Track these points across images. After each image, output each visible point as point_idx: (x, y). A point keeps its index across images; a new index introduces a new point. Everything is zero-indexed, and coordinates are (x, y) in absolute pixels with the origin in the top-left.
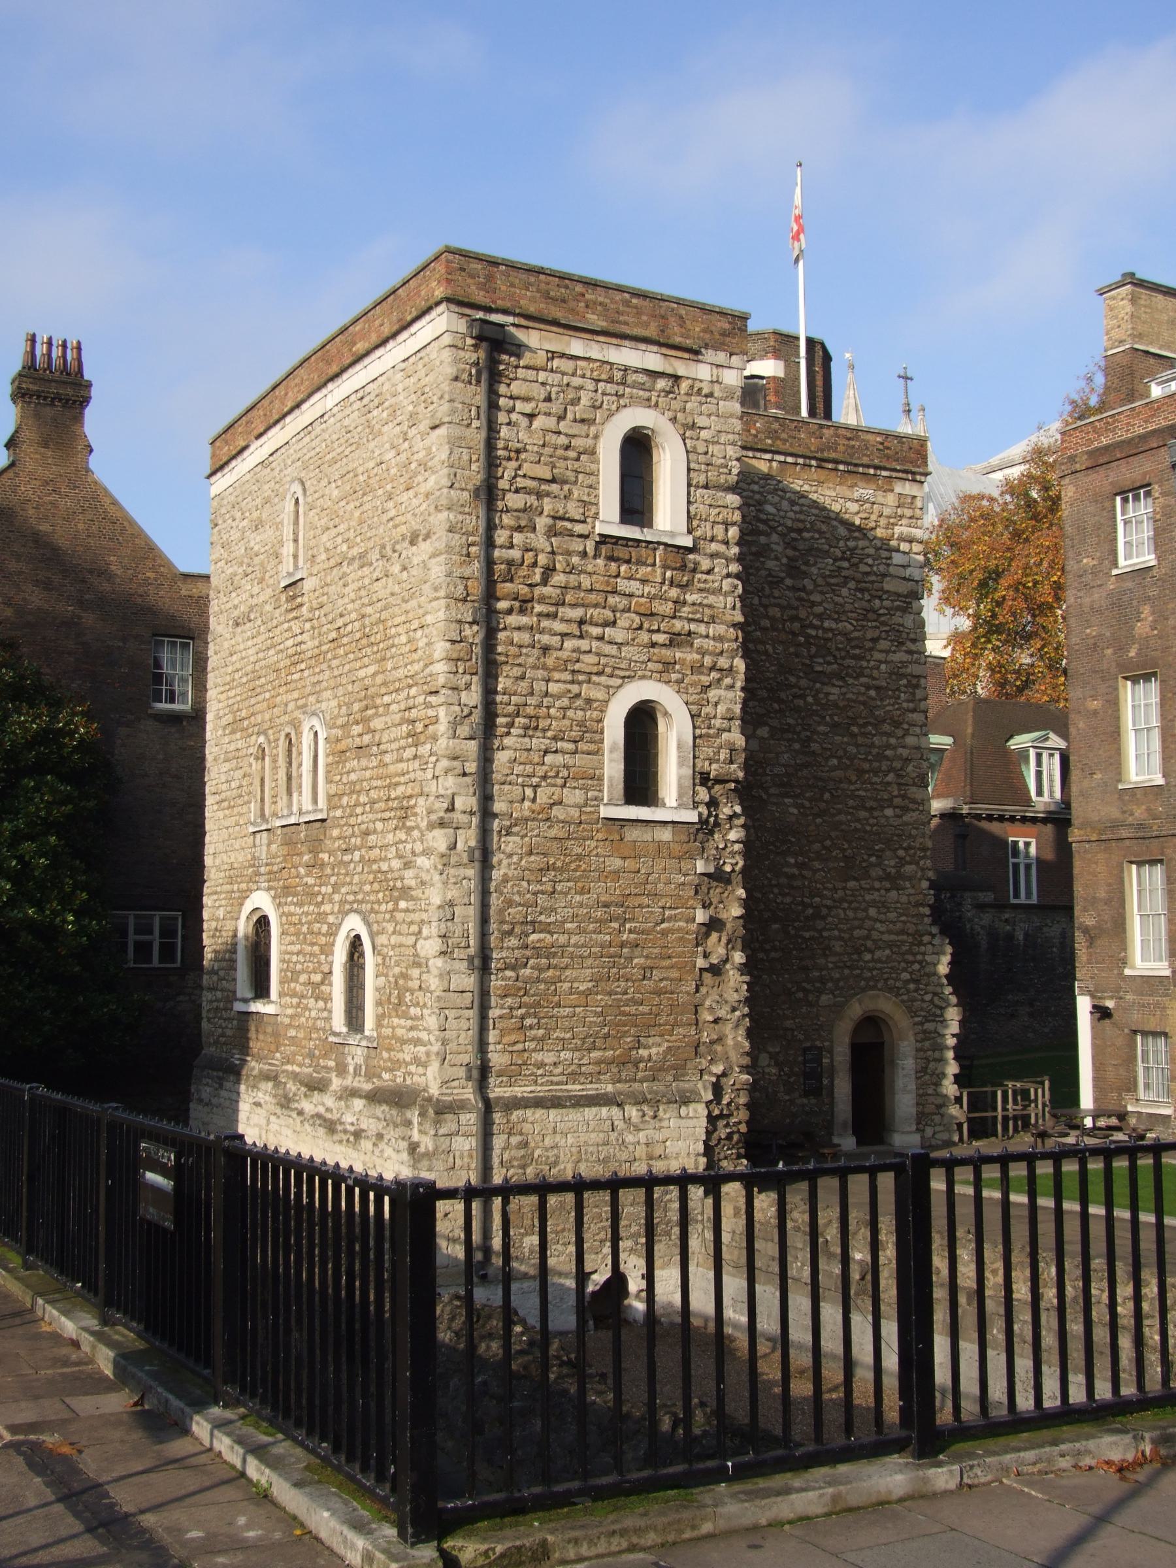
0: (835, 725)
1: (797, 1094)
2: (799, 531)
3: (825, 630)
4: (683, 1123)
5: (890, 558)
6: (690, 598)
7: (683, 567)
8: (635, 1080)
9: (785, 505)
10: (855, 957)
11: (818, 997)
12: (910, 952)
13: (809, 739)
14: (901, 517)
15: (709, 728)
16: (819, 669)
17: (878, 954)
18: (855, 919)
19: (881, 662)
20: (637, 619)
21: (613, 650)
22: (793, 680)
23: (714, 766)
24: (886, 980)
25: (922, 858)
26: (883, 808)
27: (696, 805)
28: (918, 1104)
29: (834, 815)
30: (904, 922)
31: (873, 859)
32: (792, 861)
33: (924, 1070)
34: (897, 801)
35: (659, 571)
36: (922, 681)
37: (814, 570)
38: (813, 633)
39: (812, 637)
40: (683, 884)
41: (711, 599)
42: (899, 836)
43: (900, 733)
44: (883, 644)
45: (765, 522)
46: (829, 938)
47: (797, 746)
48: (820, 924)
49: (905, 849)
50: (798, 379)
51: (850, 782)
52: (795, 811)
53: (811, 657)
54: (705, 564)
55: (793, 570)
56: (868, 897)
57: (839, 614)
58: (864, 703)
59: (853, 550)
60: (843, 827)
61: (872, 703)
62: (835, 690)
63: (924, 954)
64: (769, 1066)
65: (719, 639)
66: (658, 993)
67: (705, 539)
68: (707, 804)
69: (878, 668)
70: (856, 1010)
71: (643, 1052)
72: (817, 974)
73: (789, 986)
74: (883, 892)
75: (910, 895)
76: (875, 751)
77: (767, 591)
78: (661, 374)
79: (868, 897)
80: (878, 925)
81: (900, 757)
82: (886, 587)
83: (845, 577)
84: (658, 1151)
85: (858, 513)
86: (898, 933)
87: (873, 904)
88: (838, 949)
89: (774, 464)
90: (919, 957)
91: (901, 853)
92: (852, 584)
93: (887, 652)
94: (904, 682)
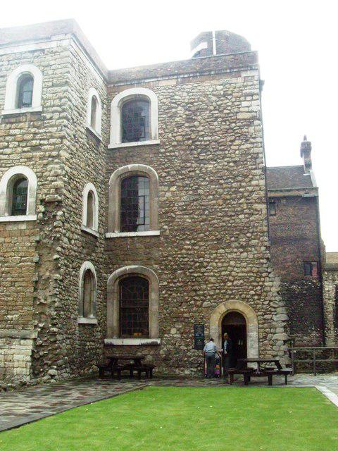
0: (211, 182)
1: (191, 347)
2: (192, 103)
3: (205, 141)
4: (20, 347)
5: (241, 104)
6: (40, 131)
7: (38, 120)
8: (5, 328)
9: (185, 94)
10: (222, 284)
11: (202, 303)
12: (255, 281)
13: (197, 189)
14: (246, 86)
15: (46, 180)
16: (202, 158)
17: (235, 283)
18: (222, 267)
19: (236, 150)
20: (17, 143)
21: (6, 157)
22: (189, 164)
23: (48, 196)
24: (241, 295)
25: (261, 236)
26: (238, 215)
27: (37, 213)
28: (260, 354)
29: (210, 221)
30: (252, 267)
31: (233, 239)
32: (189, 242)
33: (265, 338)
34: (247, 211)
35: (27, 123)
36: (260, 155)
37: (200, 117)
38: (199, 143)
39: (198, 145)
40: (30, 246)
41: (50, 129)
42: (247, 227)
43: (247, 180)
44: (237, 142)
45: (175, 103)
46: (208, 276)
47: (191, 192)
48: (203, 270)
49: (252, 233)
50: (212, 48)
51: (220, 205)
52: (190, 221)
53: (199, 154)
54: (48, 116)
55: (189, 119)
56: (229, 256)
57: (213, 133)
58: (227, 170)
59: (220, 106)
60: (216, 225)
61: (231, 169)
62: (212, 166)
63: (264, 282)
64: (176, 334)
65: (54, 144)
66: (17, 292)
67: (50, 107)
68: (44, 213)
69: (234, 153)
70: (222, 309)
71: (9, 317)
72: (201, 292)
73: (187, 298)
74: (238, 254)
75: (254, 254)
76: (232, 190)
77: (176, 130)
78: (34, 51)
79: (229, 256)
80: (236, 269)
81: (248, 191)
82: (238, 117)
83: (217, 118)
84: (10, 358)
85: (222, 90)
86: (246, 273)
87: (233, 259)
88: (212, 281)
89: (179, 80)
90: (261, 283)
91: (249, 235)
92: (220, 120)
93: (239, 145)
94: (250, 157)
